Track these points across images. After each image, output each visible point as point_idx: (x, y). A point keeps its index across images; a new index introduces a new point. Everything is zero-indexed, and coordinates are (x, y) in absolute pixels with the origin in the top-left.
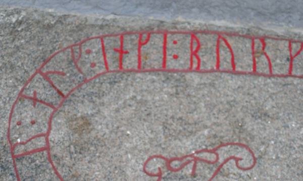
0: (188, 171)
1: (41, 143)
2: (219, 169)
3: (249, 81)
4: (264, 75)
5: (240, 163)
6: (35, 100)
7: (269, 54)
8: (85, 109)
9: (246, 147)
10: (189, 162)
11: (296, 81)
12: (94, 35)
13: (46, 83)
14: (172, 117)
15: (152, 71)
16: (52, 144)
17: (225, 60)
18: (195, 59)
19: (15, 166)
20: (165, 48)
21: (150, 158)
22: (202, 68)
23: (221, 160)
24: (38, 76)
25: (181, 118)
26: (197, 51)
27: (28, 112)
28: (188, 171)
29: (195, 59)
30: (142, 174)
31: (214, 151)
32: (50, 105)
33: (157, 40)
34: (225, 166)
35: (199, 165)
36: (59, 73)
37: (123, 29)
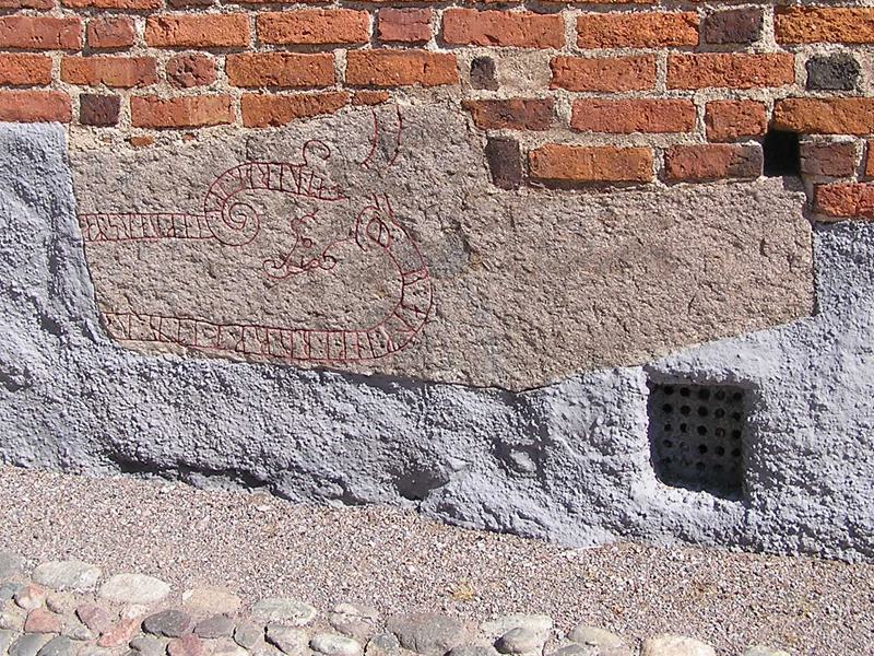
35: (299, 262)
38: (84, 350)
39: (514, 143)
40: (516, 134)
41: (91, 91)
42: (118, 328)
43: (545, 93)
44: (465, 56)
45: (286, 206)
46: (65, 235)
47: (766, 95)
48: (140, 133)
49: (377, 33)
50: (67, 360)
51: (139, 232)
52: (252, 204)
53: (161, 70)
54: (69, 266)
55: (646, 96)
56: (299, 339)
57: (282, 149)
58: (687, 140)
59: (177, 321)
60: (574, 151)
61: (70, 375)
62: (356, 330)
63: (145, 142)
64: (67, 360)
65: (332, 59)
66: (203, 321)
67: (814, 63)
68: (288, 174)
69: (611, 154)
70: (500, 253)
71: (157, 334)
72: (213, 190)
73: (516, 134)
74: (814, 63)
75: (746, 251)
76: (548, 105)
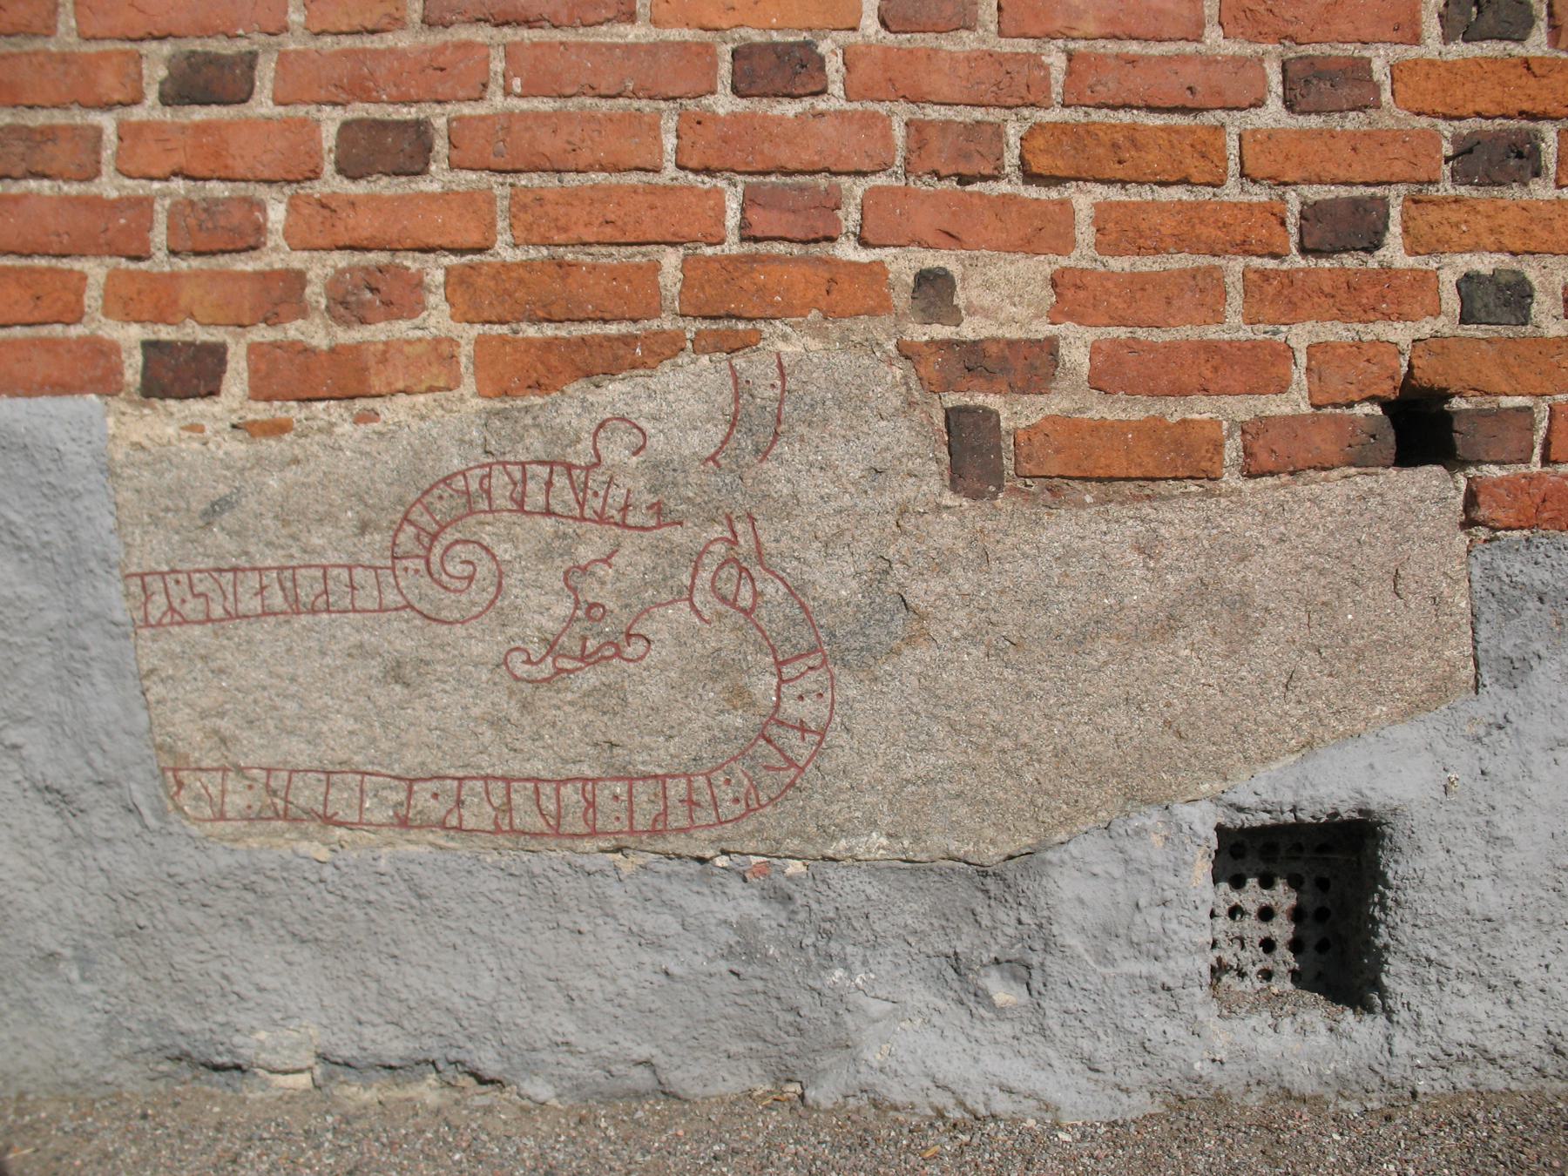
0: (592, 644)
1: (788, 671)
2: (552, 647)
3: (516, 767)
4: (495, 778)
5: (524, 657)
6: (803, 728)
7: (489, 809)
8: (736, 720)
9: (517, 679)
10: (590, 656)
11: (452, 772)
12: (729, 826)
13: (789, 754)
14: (615, 714)
15: (645, 777)
16: (774, 670)
17: (549, 798)
18: (589, 796)
19: (818, 638)
20: (631, 812)
21: (641, 658)
22: (579, 785)
23: (549, 659)
24: (801, 764)
25: (604, 713)
26: (586, 810)
27: (808, 710)
28: (592, 644)
29: (589, 796)
30: (651, 637)
31: (560, 671)
32: (781, 723)
33: (641, 822)
34: (544, 651)
35: (577, 651)
36: (774, 769)
37: (691, 837)
38: (121, 847)
39: (989, 415)
40: (993, 401)
41: (166, 333)
42: (198, 798)
43: (1043, 329)
44: (903, 264)
45: (556, 544)
46: (96, 616)
47: (1400, 333)
48: (261, 411)
49: (744, 225)
50: (84, 868)
51: (252, 604)
52: (487, 540)
53: (315, 293)
54: (99, 677)
55: (1212, 333)
56: (575, 797)
57: (556, 435)
58: (1276, 406)
59: (323, 777)
60: (1098, 427)
61: (90, 899)
62: (685, 774)
63: (278, 428)
64: (84, 868)
65: (656, 267)
66: (377, 774)
67: (1469, 283)
68: (560, 481)
69: (1152, 430)
70: (960, 615)
71: (280, 804)
72: (413, 517)
73: (993, 401)
74: (1469, 283)
75: (1370, 592)
76: (1050, 347)
